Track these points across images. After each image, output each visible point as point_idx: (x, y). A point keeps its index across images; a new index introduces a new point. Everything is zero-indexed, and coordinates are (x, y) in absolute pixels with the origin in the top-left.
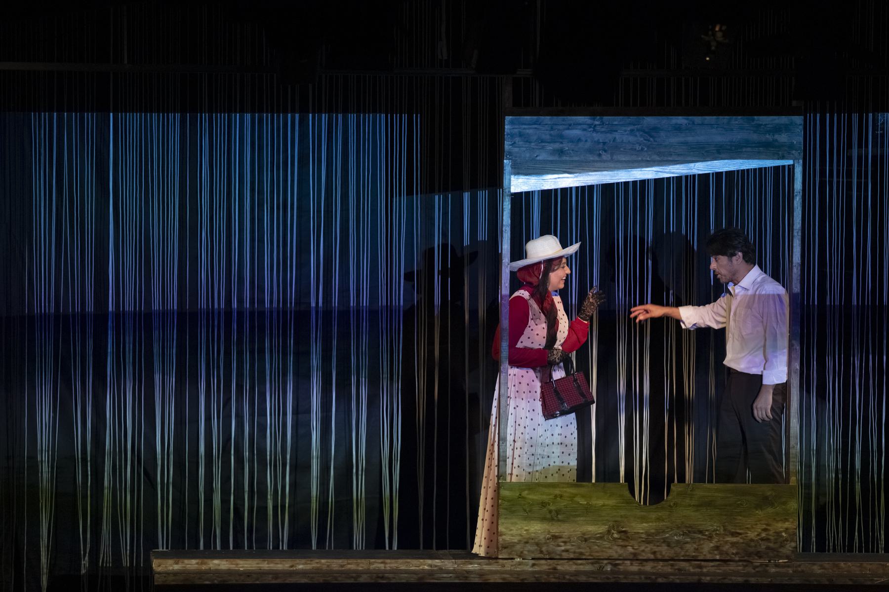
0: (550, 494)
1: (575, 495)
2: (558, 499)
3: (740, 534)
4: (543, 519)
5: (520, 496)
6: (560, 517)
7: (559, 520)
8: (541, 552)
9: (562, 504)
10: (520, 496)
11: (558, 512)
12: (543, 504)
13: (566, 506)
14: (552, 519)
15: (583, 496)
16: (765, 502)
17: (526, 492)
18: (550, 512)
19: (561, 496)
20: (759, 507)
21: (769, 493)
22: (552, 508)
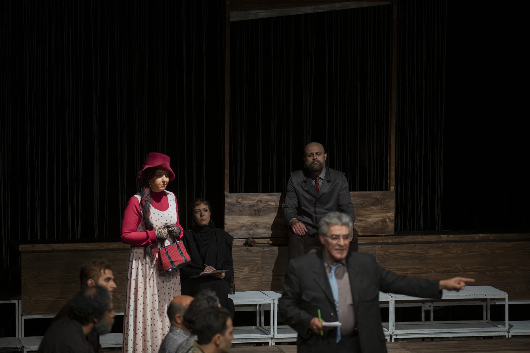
0: (254, 200)
1: (269, 201)
2: (259, 203)
3: (363, 220)
4: (250, 215)
5: (237, 202)
6: (261, 213)
7: (259, 215)
8: (250, 234)
9: (261, 205)
10: (237, 202)
11: (259, 211)
12: (251, 206)
13: (263, 207)
14: (256, 215)
15: (274, 201)
16: (377, 202)
17: (240, 199)
18: (255, 210)
19: (261, 201)
20: (373, 204)
21: (379, 197)
22: (256, 208)
